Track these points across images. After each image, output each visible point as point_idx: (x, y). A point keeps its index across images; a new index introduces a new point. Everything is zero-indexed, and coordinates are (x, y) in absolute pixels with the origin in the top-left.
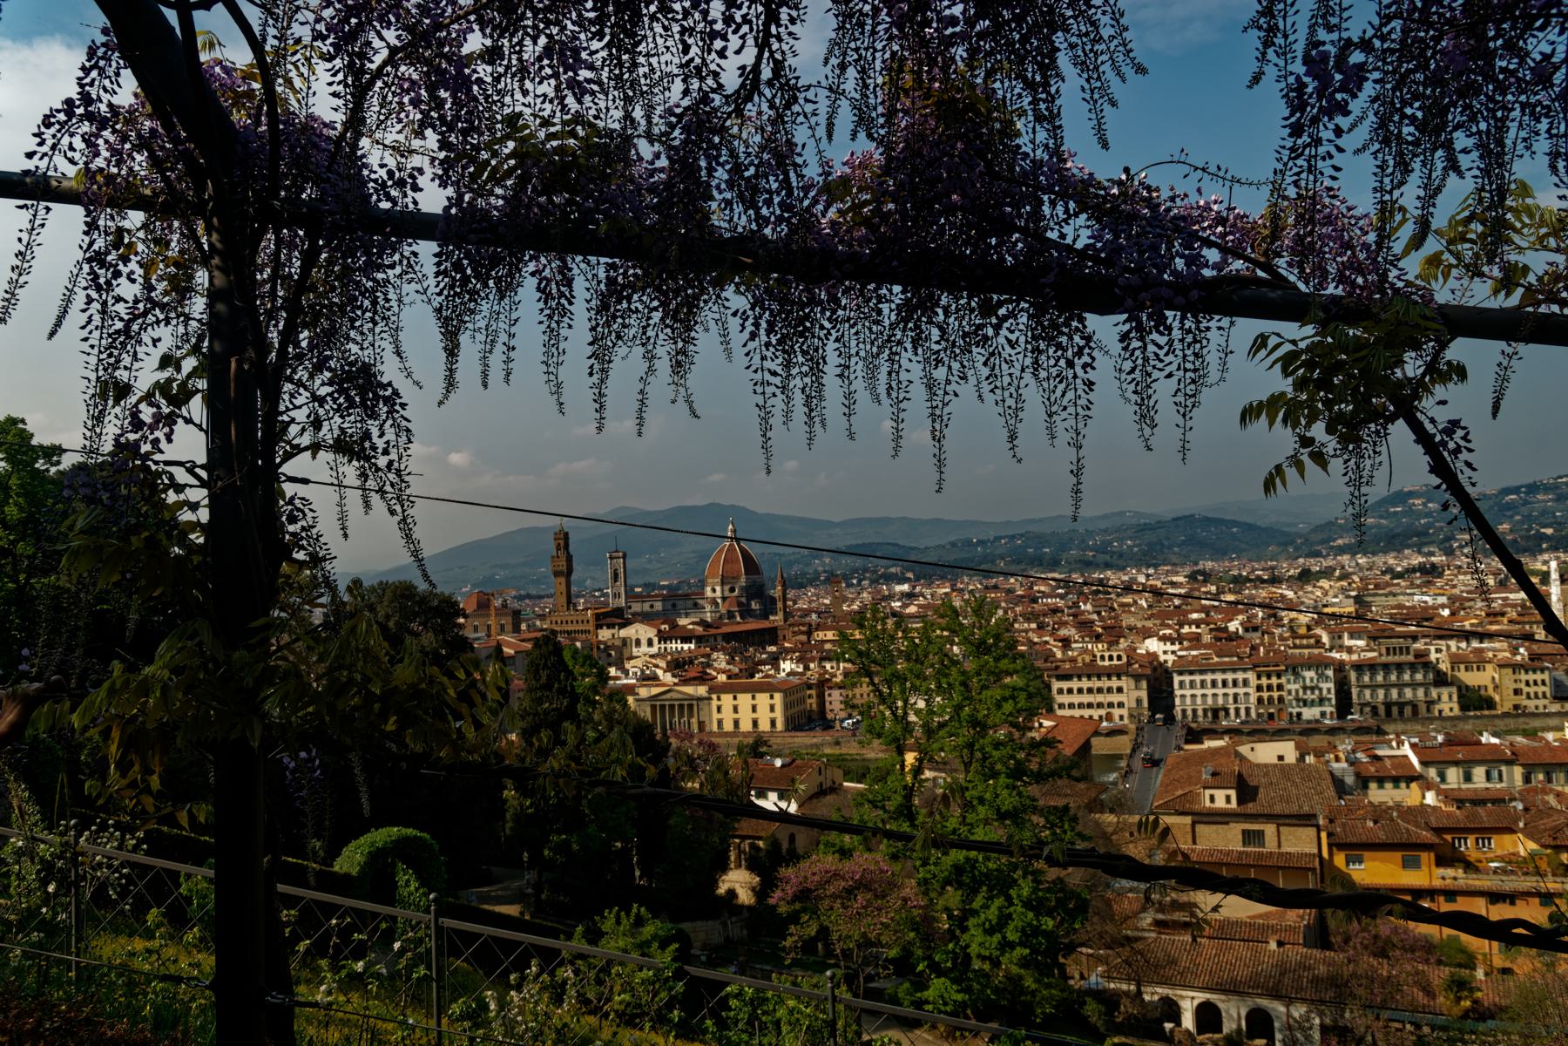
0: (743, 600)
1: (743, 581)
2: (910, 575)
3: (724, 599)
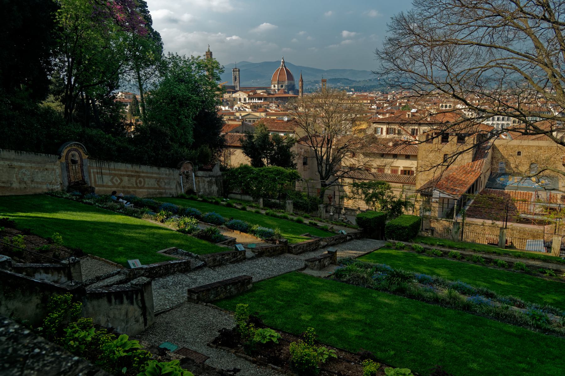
0: (286, 91)
1: (286, 83)
2: (353, 90)
3: (278, 90)
